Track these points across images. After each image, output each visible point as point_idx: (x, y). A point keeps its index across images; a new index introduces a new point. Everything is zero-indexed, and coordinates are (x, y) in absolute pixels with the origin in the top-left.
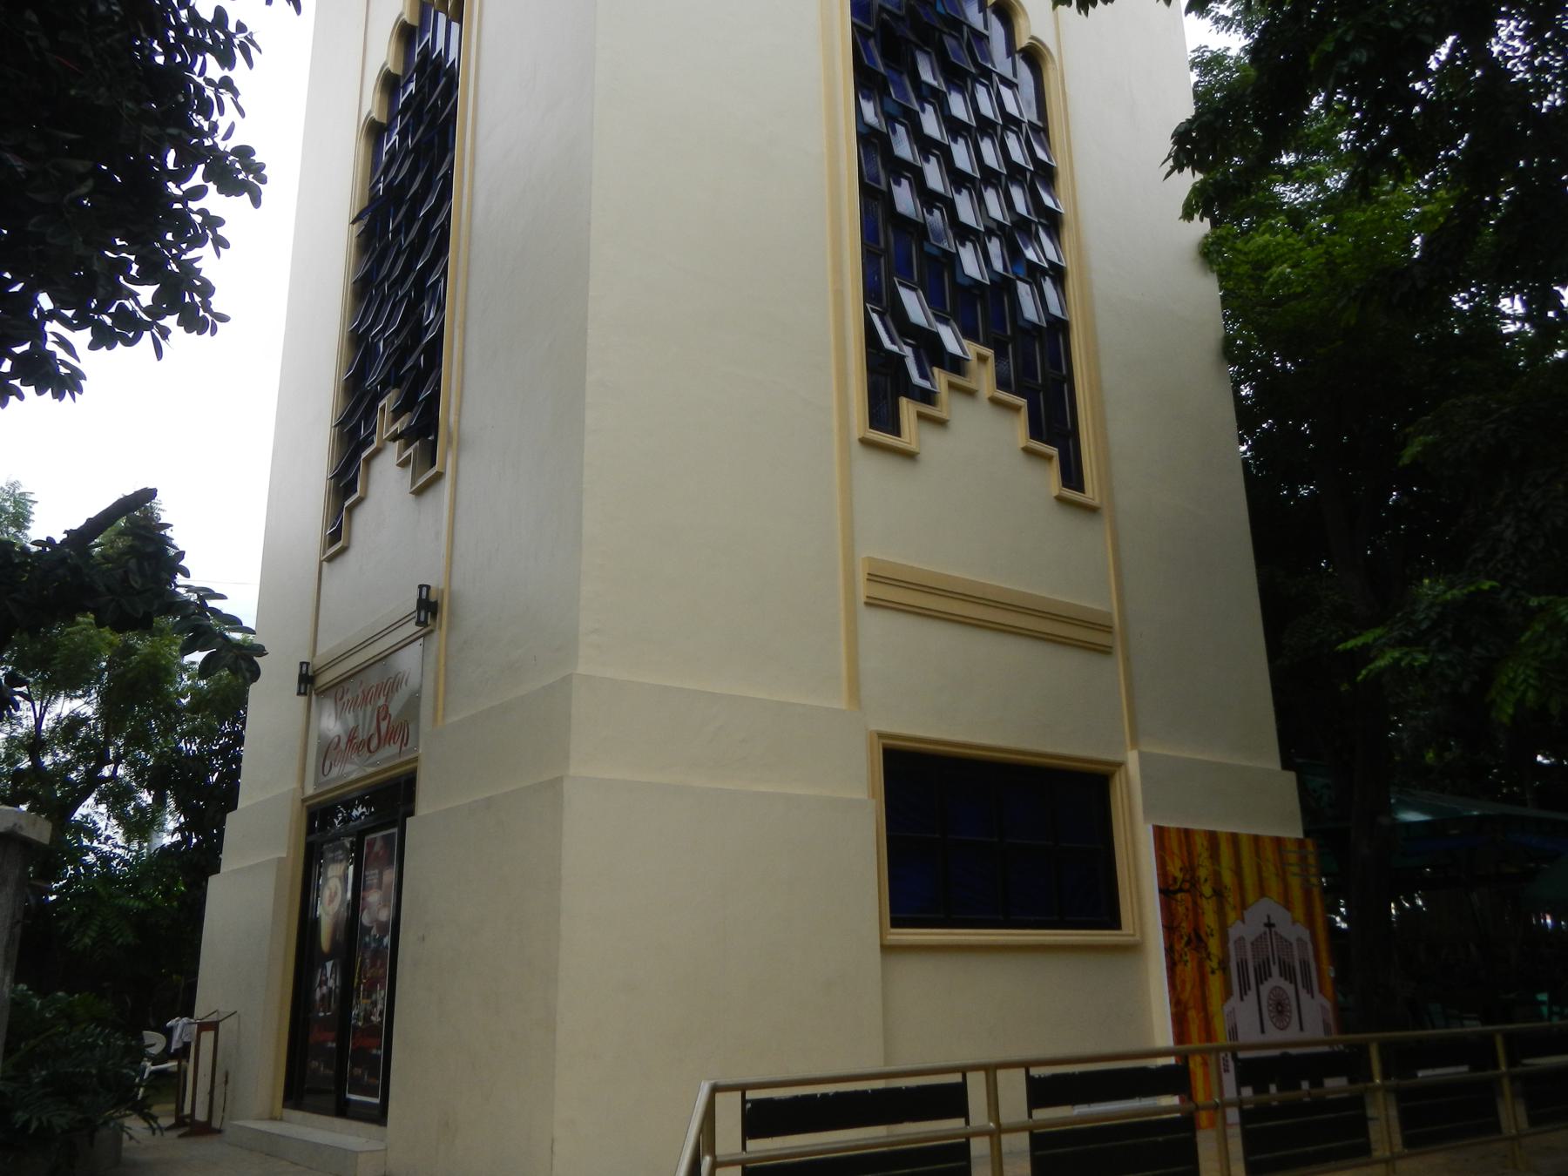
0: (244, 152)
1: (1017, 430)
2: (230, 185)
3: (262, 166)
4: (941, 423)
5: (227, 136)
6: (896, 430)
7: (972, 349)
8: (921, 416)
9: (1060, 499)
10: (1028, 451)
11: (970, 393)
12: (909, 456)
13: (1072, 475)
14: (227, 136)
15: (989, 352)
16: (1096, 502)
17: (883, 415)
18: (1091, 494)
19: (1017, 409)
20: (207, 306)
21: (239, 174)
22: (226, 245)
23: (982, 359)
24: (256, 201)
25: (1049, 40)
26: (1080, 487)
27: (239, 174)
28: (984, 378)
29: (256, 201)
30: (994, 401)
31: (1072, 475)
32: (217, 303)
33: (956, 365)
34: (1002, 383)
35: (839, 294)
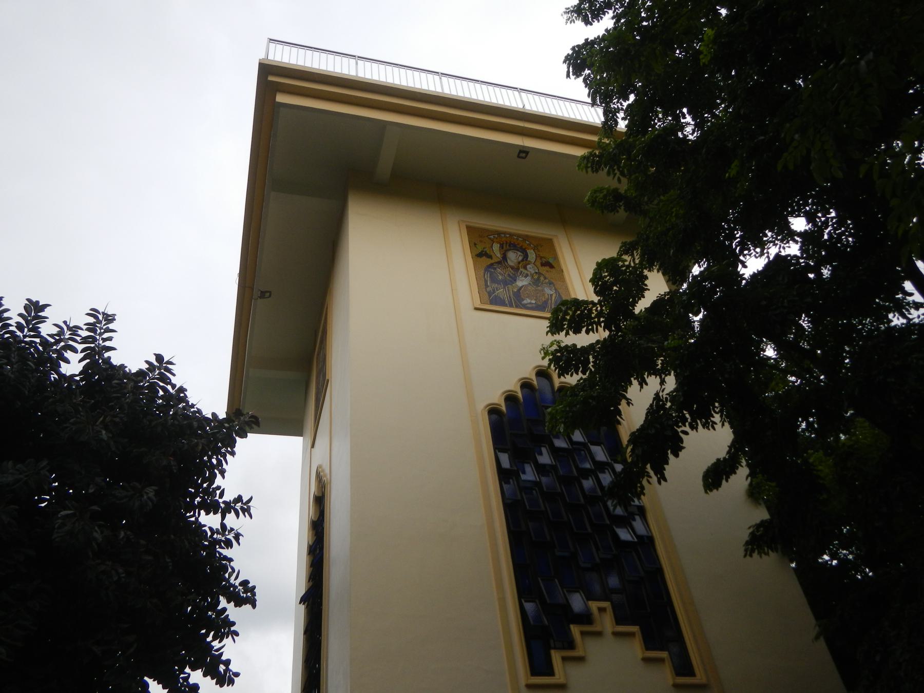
0: (245, 583)
1: (635, 649)
2: (239, 602)
3: (254, 587)
4: (581, 659)
5: (236, 579)
6: (551, 673)
8: (564, 659)
9: (676, 686)
10: (646, 660)
11: (599, 634)
12: (562, 687)
13: (683, 667)
14: (236, 579)
16: (704, 681)
17: (539, 665)
18: (700, 677)
19: (631, 635)
20: (227, 670)
21: (245, 596)
22: (237, 634)
23: (602, 610)
24: (254, 606)
26: (692, 673)
27: (245, 596)
28: (607, 622)
29: (254, 606)
30: (616, 634)
31: (683, 667)
32: (233, 667)
33: (585, 618)
34: (619, 621)
35: (502, 600)
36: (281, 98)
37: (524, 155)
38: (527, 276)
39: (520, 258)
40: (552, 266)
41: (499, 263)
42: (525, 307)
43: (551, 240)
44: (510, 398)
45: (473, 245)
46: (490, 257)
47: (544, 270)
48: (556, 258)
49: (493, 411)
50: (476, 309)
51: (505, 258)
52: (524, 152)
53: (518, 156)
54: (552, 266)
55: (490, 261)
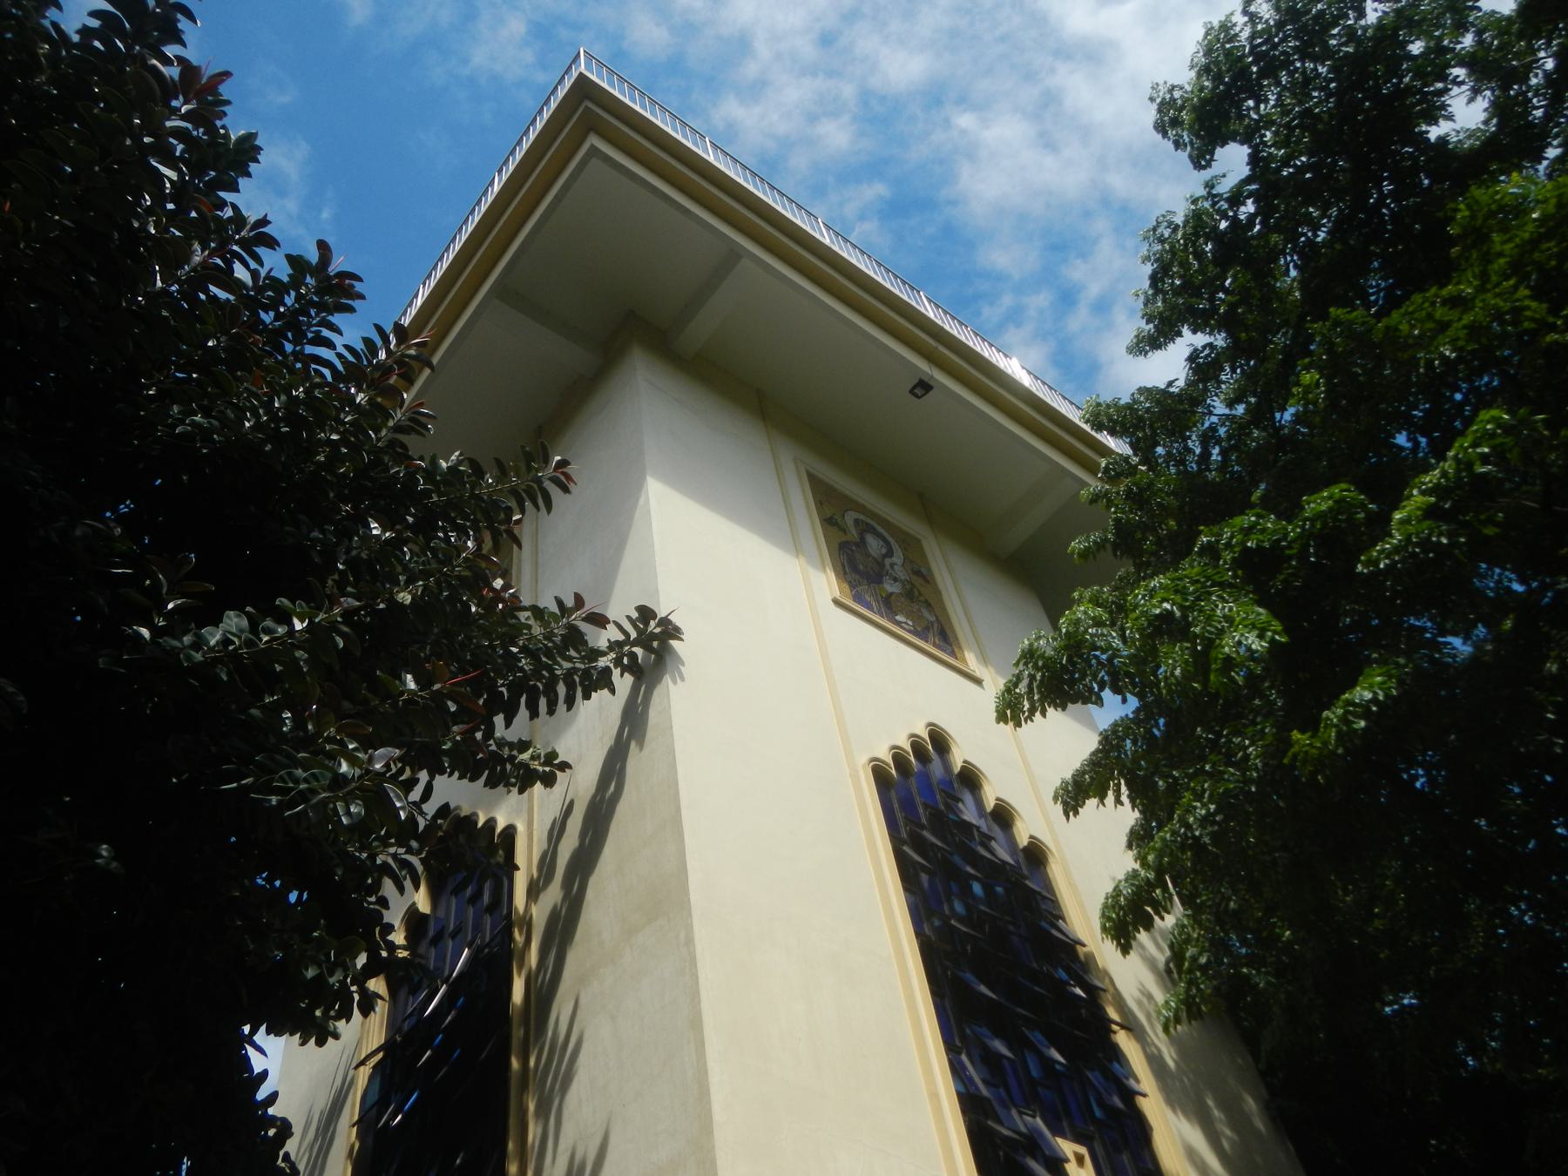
7: (1067, 1147)
15: (1083, 1150)
25: (1046, 838)
35: (934, 1096)
36: (594, 140)
37: (918, 391)
38: (895, 580)
39: (884, 551)
40: (927, 582)
41: (857, 545)
42: (898, 624)
43: (919, 541)
44: (899, 758)
45: (820, 504)
46: (844, 531)
47: (917, 581)
48: (929, 570)
49: (879, 773)
50: (837, 602)
51: (863, 539)
52: (923, 387)
53: (912, 392)
54: (927, 582)
55: (844, 539)
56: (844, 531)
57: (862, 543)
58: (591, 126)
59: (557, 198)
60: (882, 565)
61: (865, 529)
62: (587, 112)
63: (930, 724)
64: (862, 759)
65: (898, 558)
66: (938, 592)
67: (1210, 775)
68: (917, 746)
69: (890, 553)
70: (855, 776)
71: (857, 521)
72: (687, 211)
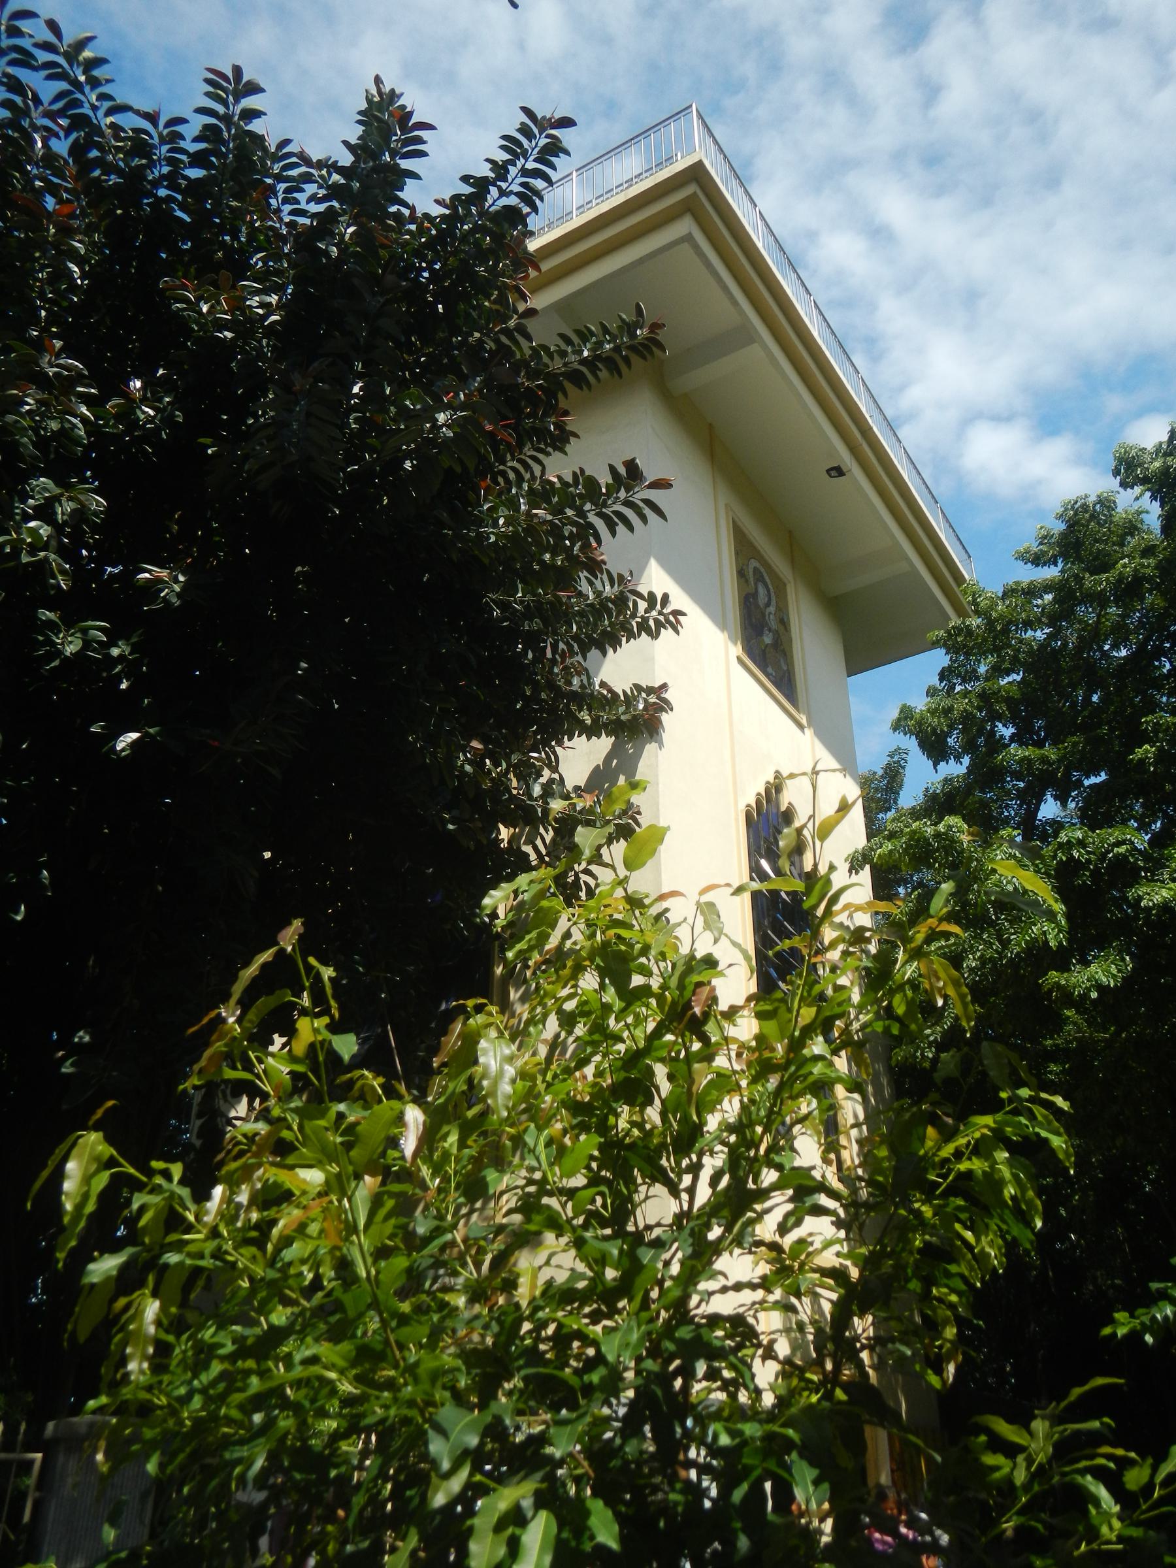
37: (833, 473)
38: (770, 630)
43: (785, 585)
49: (748, 815)
50: (739, 659)
51: (756, 589)
52: (838, 471)
53: (828, 471)
56: (747, 581)
57: (755, 595)
58: (688, 208)
59: (641, 261)
60: (763, 615)
61: (759, 578)
62: (693, 198)
63: (777, 772)
64: (742, 808)
65: (772, 609)
66: (790, 640)
67: (985, 942)
68: (767, 790)
69: (768, 605)
70: (737, 820)
71: (755, 569)
72: (725, 288)
